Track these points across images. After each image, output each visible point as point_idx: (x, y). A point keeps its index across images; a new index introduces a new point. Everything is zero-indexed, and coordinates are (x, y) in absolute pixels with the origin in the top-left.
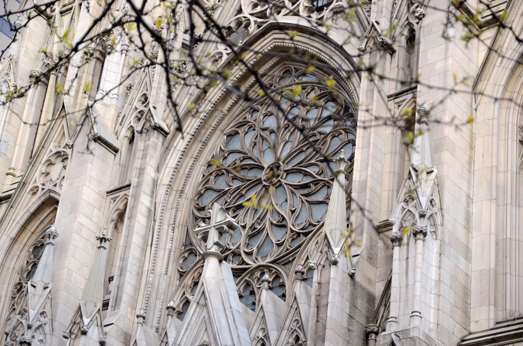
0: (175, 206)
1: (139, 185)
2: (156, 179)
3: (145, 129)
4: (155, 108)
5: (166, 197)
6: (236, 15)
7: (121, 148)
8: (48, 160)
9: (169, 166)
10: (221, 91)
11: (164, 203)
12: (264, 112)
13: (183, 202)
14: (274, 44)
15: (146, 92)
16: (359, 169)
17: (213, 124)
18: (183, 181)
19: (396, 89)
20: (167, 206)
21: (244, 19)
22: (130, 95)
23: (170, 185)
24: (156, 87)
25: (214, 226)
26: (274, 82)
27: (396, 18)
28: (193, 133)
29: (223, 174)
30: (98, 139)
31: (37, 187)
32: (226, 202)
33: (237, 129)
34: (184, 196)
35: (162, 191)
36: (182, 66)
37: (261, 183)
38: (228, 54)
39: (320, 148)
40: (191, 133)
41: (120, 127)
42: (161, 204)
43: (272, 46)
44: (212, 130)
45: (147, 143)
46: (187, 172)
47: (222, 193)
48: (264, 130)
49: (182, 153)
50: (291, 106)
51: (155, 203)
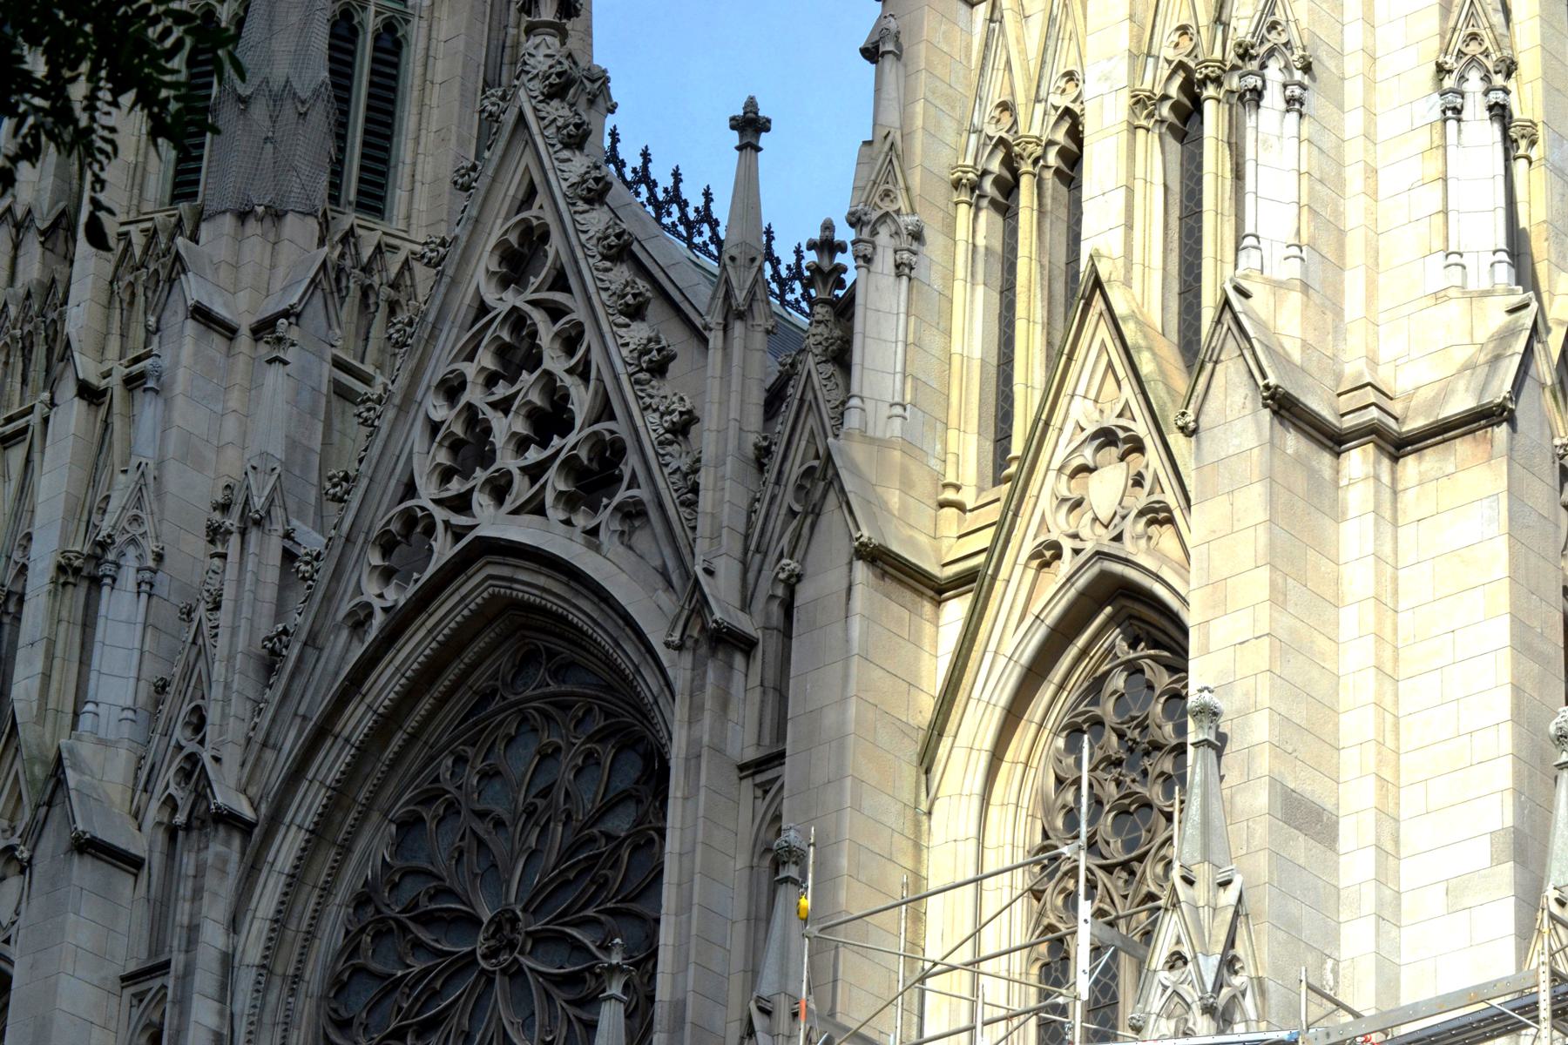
0: (280, 1017)
1: (189, 971)
2: (230, 951)
3: (197, 818)
4: (217, 760)
5: (256, 999)
6: (401, 502)
7: (150, 857)
9: (259, 914)
10: (370, 713)
11: (253, 1014)
13: (301, 1006)
14: (490, 590)
15: (200, 702)
16: (669, 969)
17: (361, 798)
18: (297, 950)
19: (759, 744)
20: (260, 1020)
22: (165, 708)
23: (263, 966)
24: (220, 697)
26: (499, 683)
27: (757, 550)
28: (311, 827)
29: (390, 930)
30: (88, 847)
32: (400, 1009)
33: (418, 808)
34: (303, 986)
35: (245, 981)
36: (280, 640)
37: (475, 962)
38: (385, 610)
39: (605, 875)
40: (306, 826)
41: (145, 797)
42: (245, 1019)
43: (485, 595)
44: (359, 813)
45: (203, 855)
46: (304, 927)
47: (391, 985)
48: (482, 815)
49: (289, 880)
50: (539, 753)
51: (232, 1015)
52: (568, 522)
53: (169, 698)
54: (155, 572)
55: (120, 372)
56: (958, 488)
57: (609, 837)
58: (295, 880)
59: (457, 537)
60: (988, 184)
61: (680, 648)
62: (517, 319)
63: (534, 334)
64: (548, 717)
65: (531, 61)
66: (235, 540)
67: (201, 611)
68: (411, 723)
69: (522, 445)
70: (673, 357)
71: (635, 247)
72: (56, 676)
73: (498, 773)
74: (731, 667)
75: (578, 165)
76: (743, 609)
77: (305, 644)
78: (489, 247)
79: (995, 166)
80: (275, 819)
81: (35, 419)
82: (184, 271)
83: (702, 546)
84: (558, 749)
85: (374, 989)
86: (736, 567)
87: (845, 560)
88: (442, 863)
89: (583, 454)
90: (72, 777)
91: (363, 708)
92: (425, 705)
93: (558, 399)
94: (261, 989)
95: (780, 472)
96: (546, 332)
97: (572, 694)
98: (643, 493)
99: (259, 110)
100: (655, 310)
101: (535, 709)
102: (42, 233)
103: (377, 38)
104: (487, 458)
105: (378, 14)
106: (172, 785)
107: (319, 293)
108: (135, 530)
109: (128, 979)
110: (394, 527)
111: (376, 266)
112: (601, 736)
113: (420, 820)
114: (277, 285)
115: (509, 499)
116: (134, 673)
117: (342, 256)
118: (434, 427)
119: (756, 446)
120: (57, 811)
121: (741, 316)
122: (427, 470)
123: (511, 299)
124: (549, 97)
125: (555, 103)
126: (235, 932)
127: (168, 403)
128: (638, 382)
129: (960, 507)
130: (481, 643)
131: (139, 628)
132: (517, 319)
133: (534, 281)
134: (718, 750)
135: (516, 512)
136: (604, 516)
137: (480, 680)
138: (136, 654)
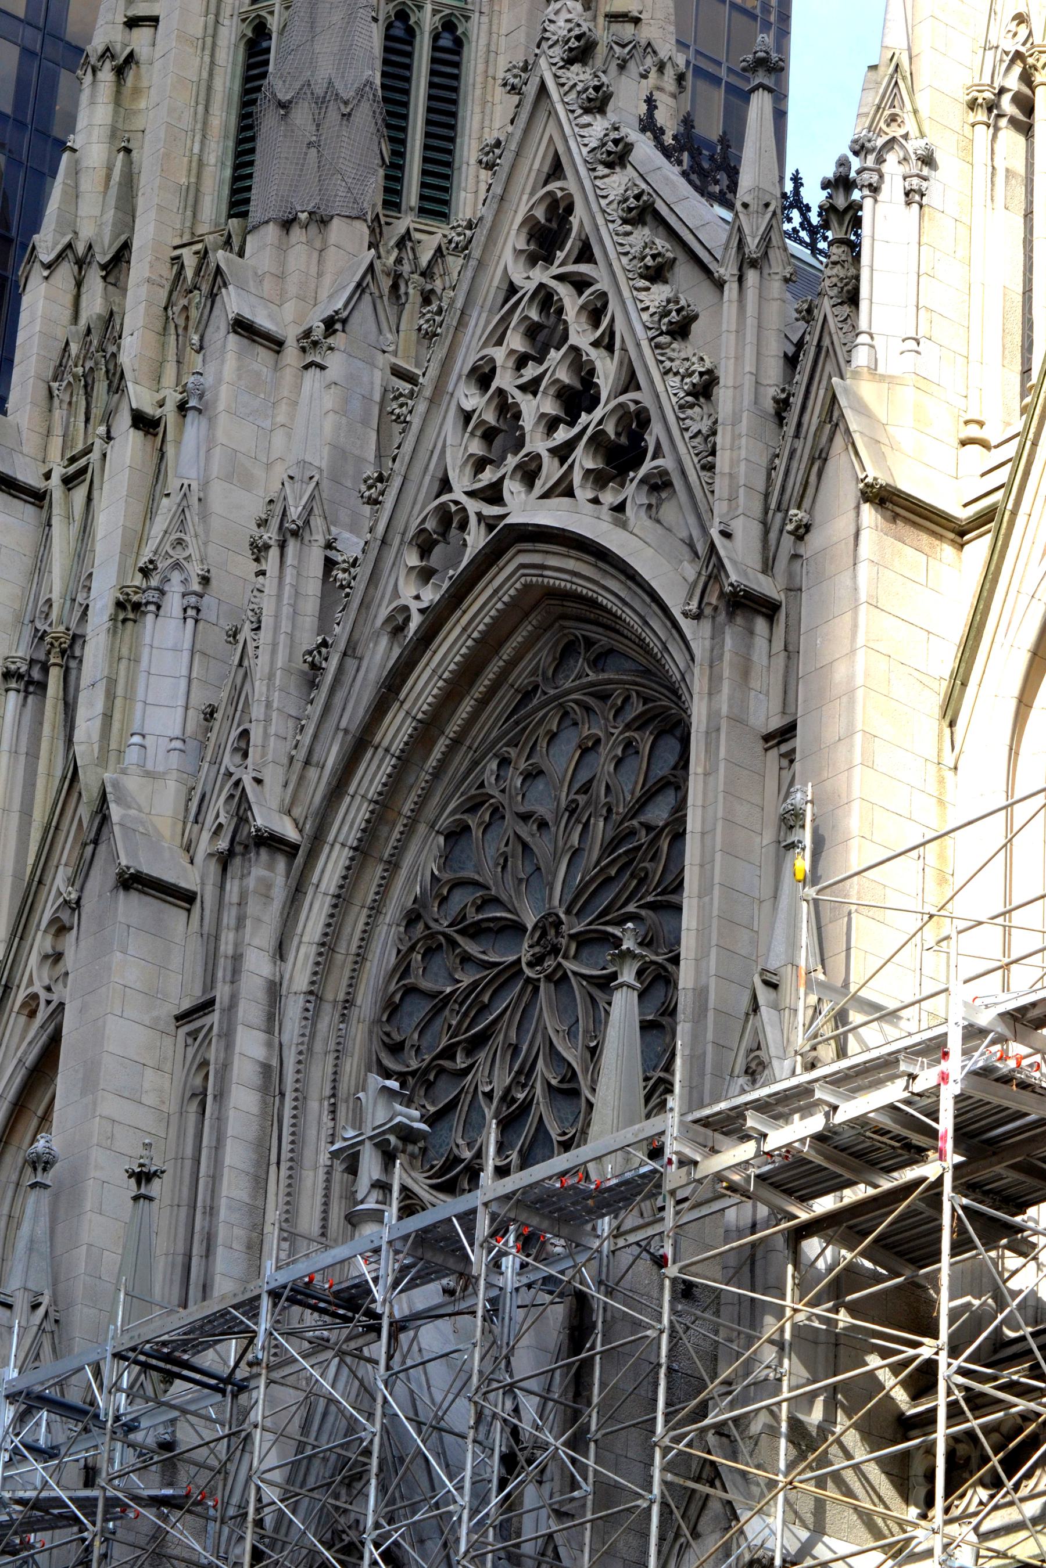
0: (332, 1046)
2: (277, 980)
3: (240, 844)
4: (259, 781)
5: (305, 1027)
6: (438, 496)
7: (202, 890)
8: (54, 920)
10: (410, 720)
11: (302, 1043)
12: (522, 766)
13: (353, 1033)
14: (523, 580)
15: (246, 726)
16: (692, 955)
17: (406, 810)
18: (347, 973)
19: (784, 713)
20: (310, 1049)
21: (453, 508)
22: (213, 736)
23: (311, 993)
24: (262, 718)
25: (371, 1138)
26: (540, 679)
27: (778, 509)
28: (355, 844)
29: (440, 946)
31: (35, 997)
32: (450, 1026)
33: (465, 817)
34: (355, 1012)
35: (293, 1009)
36: (320, 653)
37: (521, 971)
38: (421, 611)
39: (645, 868)
40: (349, 843)
41: (196, 827)
42: (293, 1048)
43: (518, 585)
44: (405, 826)
45: (245, 882)
46: (353, 949)
47: (441, 1002)
48: (525, 817)
49: (334, 901)
50: (580, 747)
51: (281, 1045)
52: (596, 501)
53: (216, 725)
54: (201, 596)
55: (173, 398)
56: (981, 424)
57: (649, 828)
58: (341, 900)
59: (490, 528)
60: (1006, 100)
61: (698, 617)
62: (545, 298)
63: (560, 311)
64: (588, 709)
65: (552, 28)
66: (274, 553)
67: (246, 632)
68: (453, 728)
69: (552, 425)
70: (695, 317)
71: (660, 206)
72: (117, 716)
73: (541, 772)
74: (751, 632)
75: (598, 127)
76: (764, 572)
77: (345, 654)
78: (516, 226)
79: (1013, 82)
80: (318, 838)
81: (95, 456)
82: (225, 285)
83: (720, 508)
84: (598, 741)
85: (425, 1007)
86: (756, 529)
87: (853, 505)
88: (488, 874)
89: (610, 429)
90: (115, 812)
91: (401, 715)
92: (466, 708)
93: (586, 374)
94: (311, 1018)
95: (799, 425)
96: (571, 303)
97: (610, 682)
98: (666, 462)
99: (302, 116)
100: (684, 273)
101: (576, 701)
102: (103, 267)
103: (436, 37)
104: (520, 443)
105: (435, 12)
106: (222, 814)
107: (367, 298)
108: (179, 554)
109: (183, 1018)
110: (430, 525)
111: (438, 270)
112: (640, 723)
113: (467, 828)
114: (323, 294)
115: (538, 483)
116: (181, 702)
117: (399, 261)
118: (467, 416)
119: (776, 401)
120: (102, 848)
121: (754, 264)
122: (459, 463)
123: (541, 275)
124: (569, 62)
125: (576, 68)
126: (282, 958)
127: (212, 421)
128: (658, 346)
129: (985, 444)
130: (518, 638)
131: (186, 655)
132: (545, 298)
133: (560, 255)
134: (738, 720)
135: (545, 496)
136: (630, 489)
137: (521, 677)
138: (183, 683)
